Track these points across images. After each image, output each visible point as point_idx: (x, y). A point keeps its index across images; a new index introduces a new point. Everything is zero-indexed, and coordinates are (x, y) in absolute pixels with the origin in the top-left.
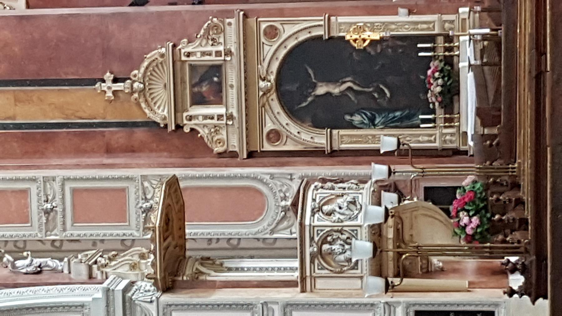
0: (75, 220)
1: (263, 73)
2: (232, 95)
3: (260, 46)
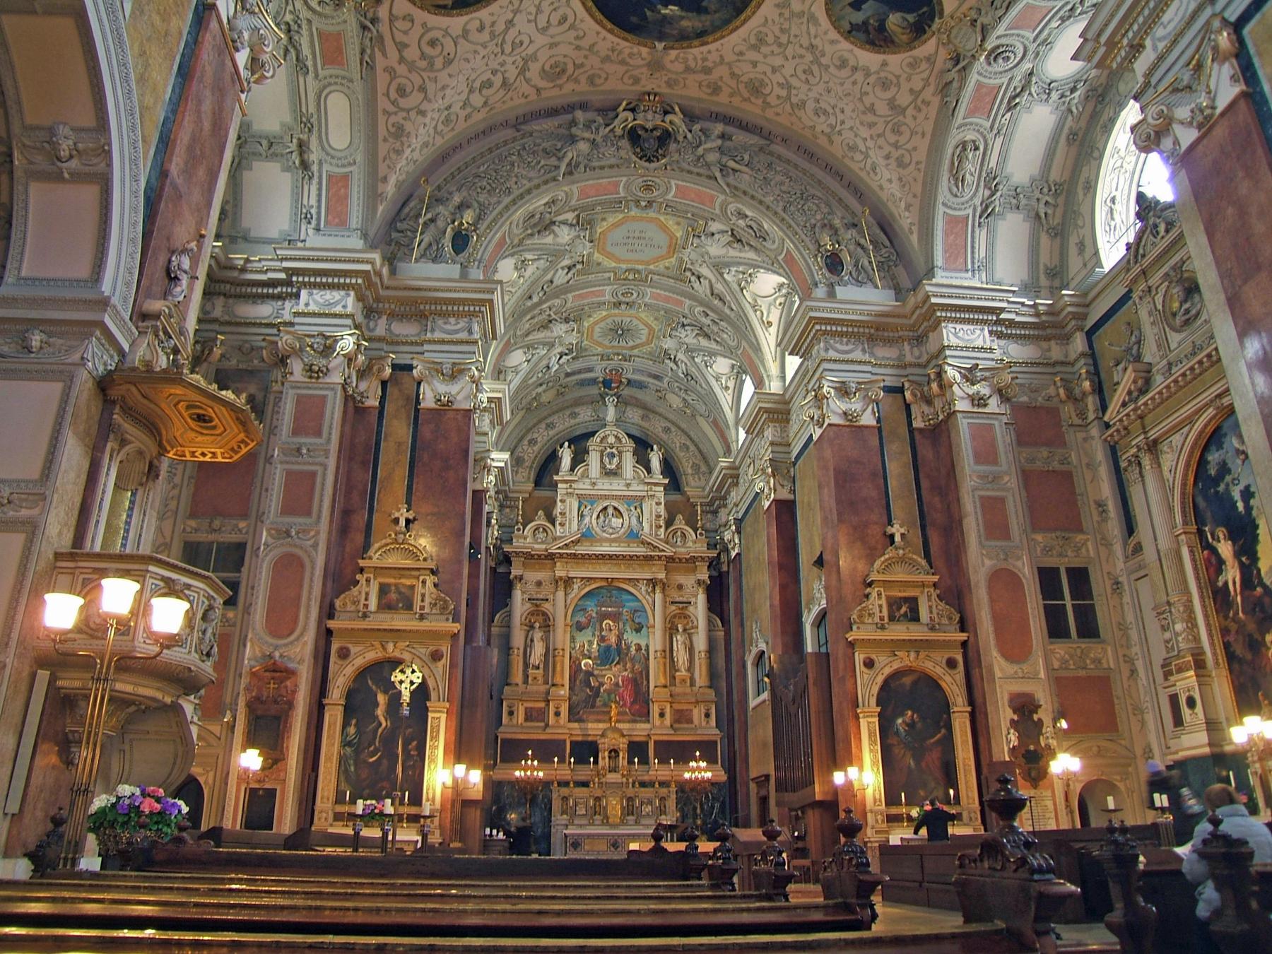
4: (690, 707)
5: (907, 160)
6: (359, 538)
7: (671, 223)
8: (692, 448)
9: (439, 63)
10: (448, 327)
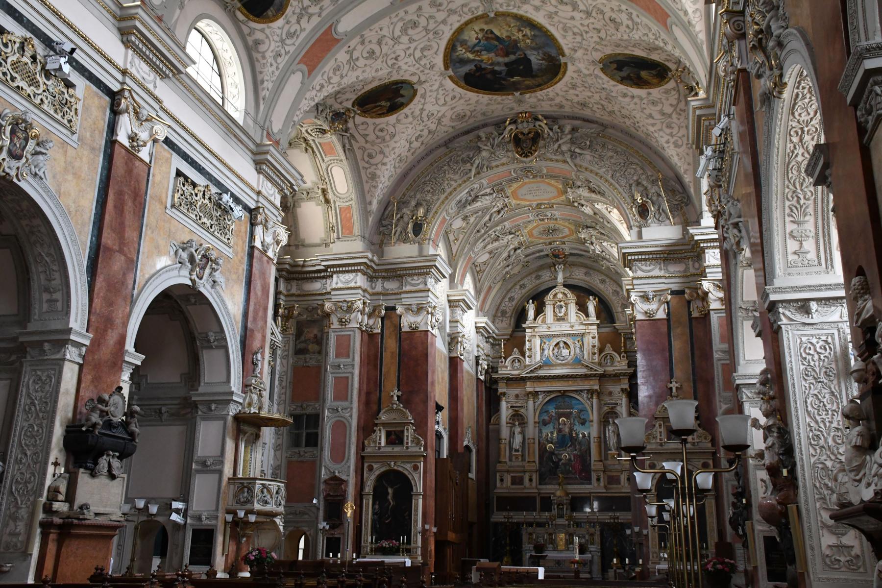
0: (336, 378)
1: (399, 464)
2: (389, 449)
3: (408, 462)
4: (619, 474)
5: (680, 143)
6: (375, 407)
7: (553, 182)
9: (387, 138)
10: (413, 282)
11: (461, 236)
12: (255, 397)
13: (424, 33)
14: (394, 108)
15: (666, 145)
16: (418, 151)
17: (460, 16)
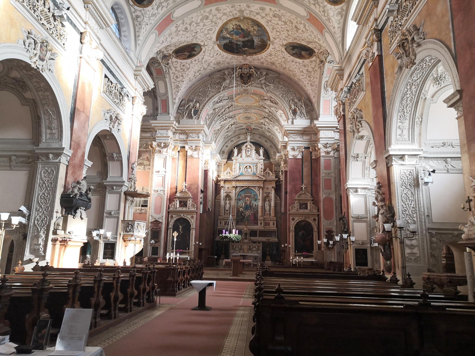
2: (181, 209)
3: (190, 215)
5: (313, 84)
7: (254, 96)
8: (273, 147)
9: (186, 70)
11: (211, 117)
12: (133, 184)
13: (210, 22)
14: (190, 56)
15: (307, 85)
16: (198, 77)
17: (228, 16)
